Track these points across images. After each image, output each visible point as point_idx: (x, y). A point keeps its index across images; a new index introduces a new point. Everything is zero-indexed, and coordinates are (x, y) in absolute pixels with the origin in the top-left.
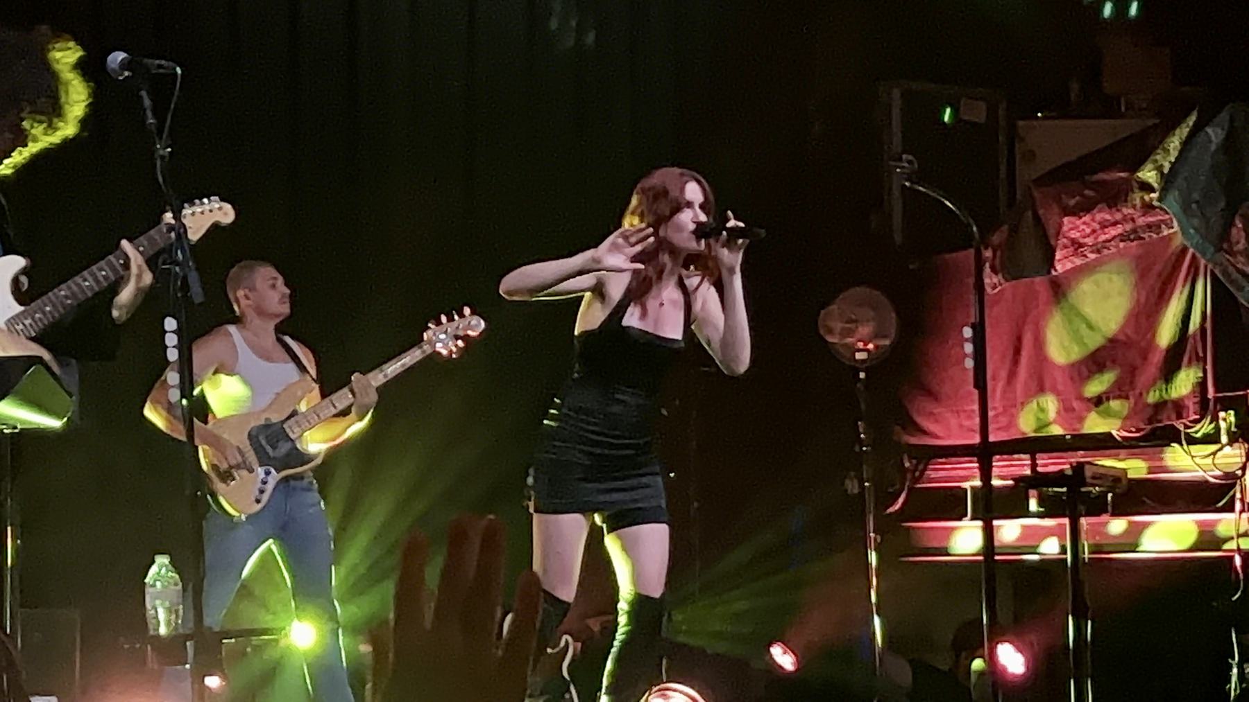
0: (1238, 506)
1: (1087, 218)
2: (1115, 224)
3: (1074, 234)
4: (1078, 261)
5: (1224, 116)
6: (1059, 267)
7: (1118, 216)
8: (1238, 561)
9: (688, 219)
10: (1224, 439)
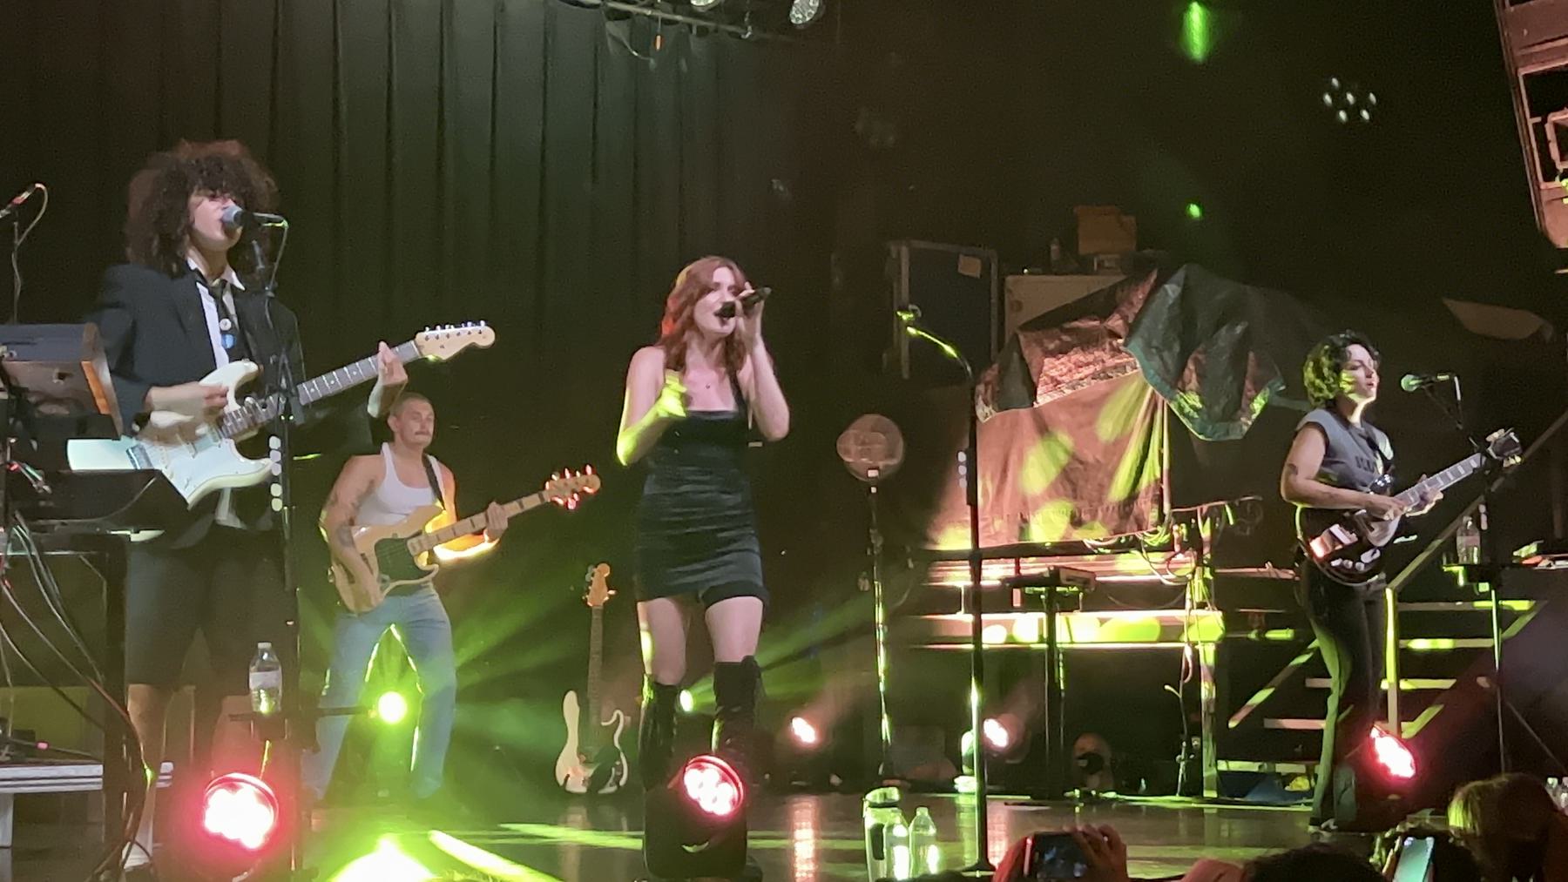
1: (1064, 359)
2: (1088, 364)
3: (1054, 373)
4: (1056, 396)
5: (1180, 275)
6: (1039, 399)
7: (1090, 358)
8: (1188, 653)
9: (714, 300)
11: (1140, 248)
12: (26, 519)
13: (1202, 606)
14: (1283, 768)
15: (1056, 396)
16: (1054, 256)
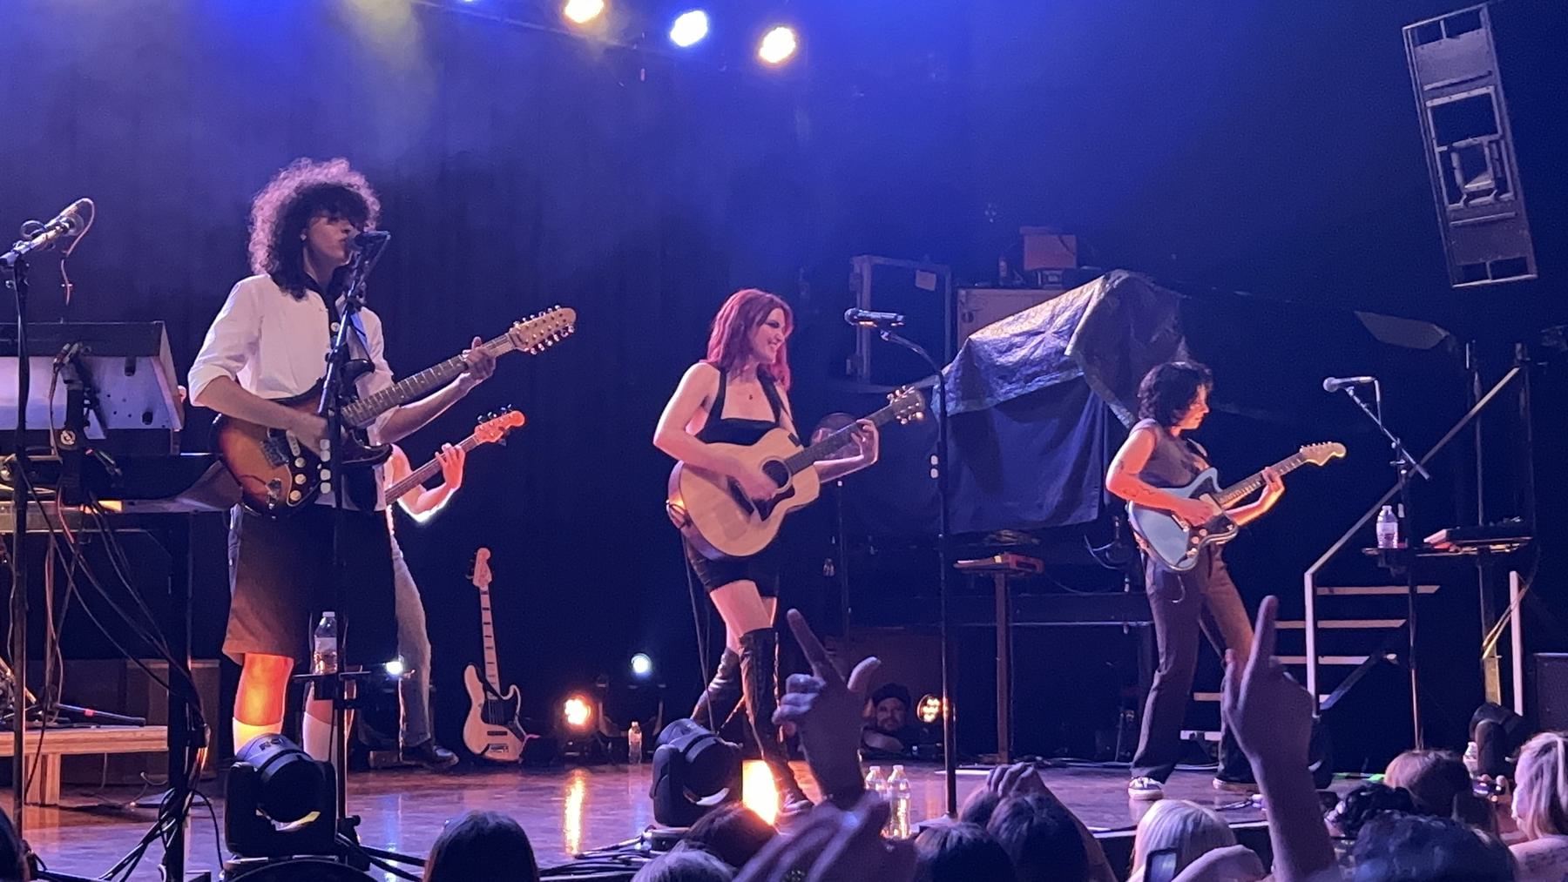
11: (1079, 265)
16: (1003, 274)
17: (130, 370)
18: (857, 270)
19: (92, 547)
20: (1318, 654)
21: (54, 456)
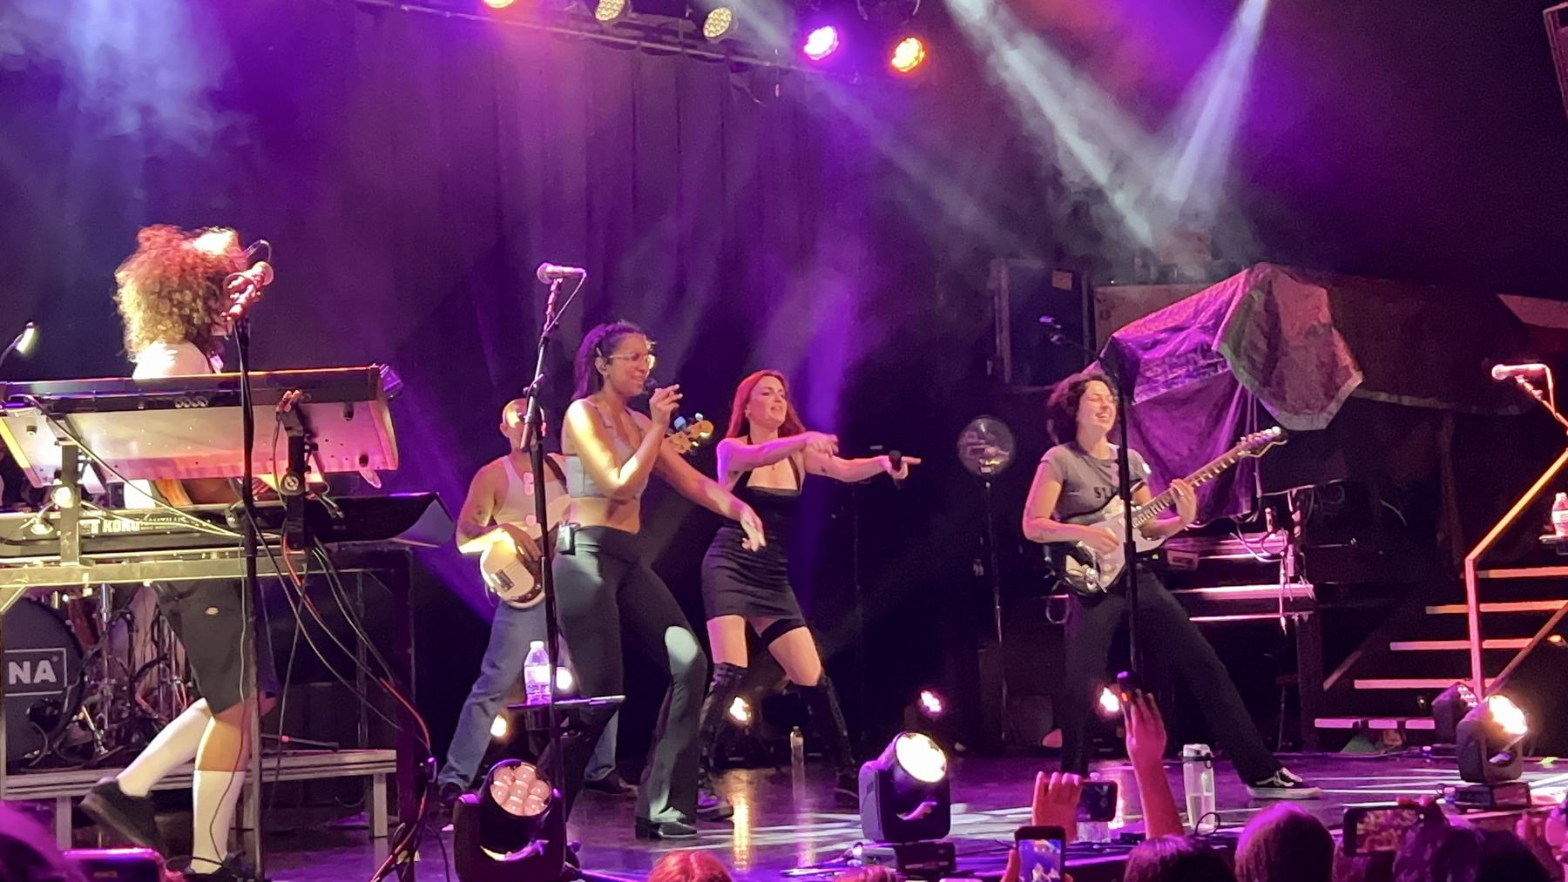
0: (1282, 579)
2: (1182, 365)
3: (1149, 374)
10: (1270, 528)
12: (323, 541)
13: (1294, 580)
14: (1374, 724)
15: (1153, 395)
17: (350, 415)
18: (994, 273)
19: (317, 587)
20: (1484, 635)
21: (281, 502)
